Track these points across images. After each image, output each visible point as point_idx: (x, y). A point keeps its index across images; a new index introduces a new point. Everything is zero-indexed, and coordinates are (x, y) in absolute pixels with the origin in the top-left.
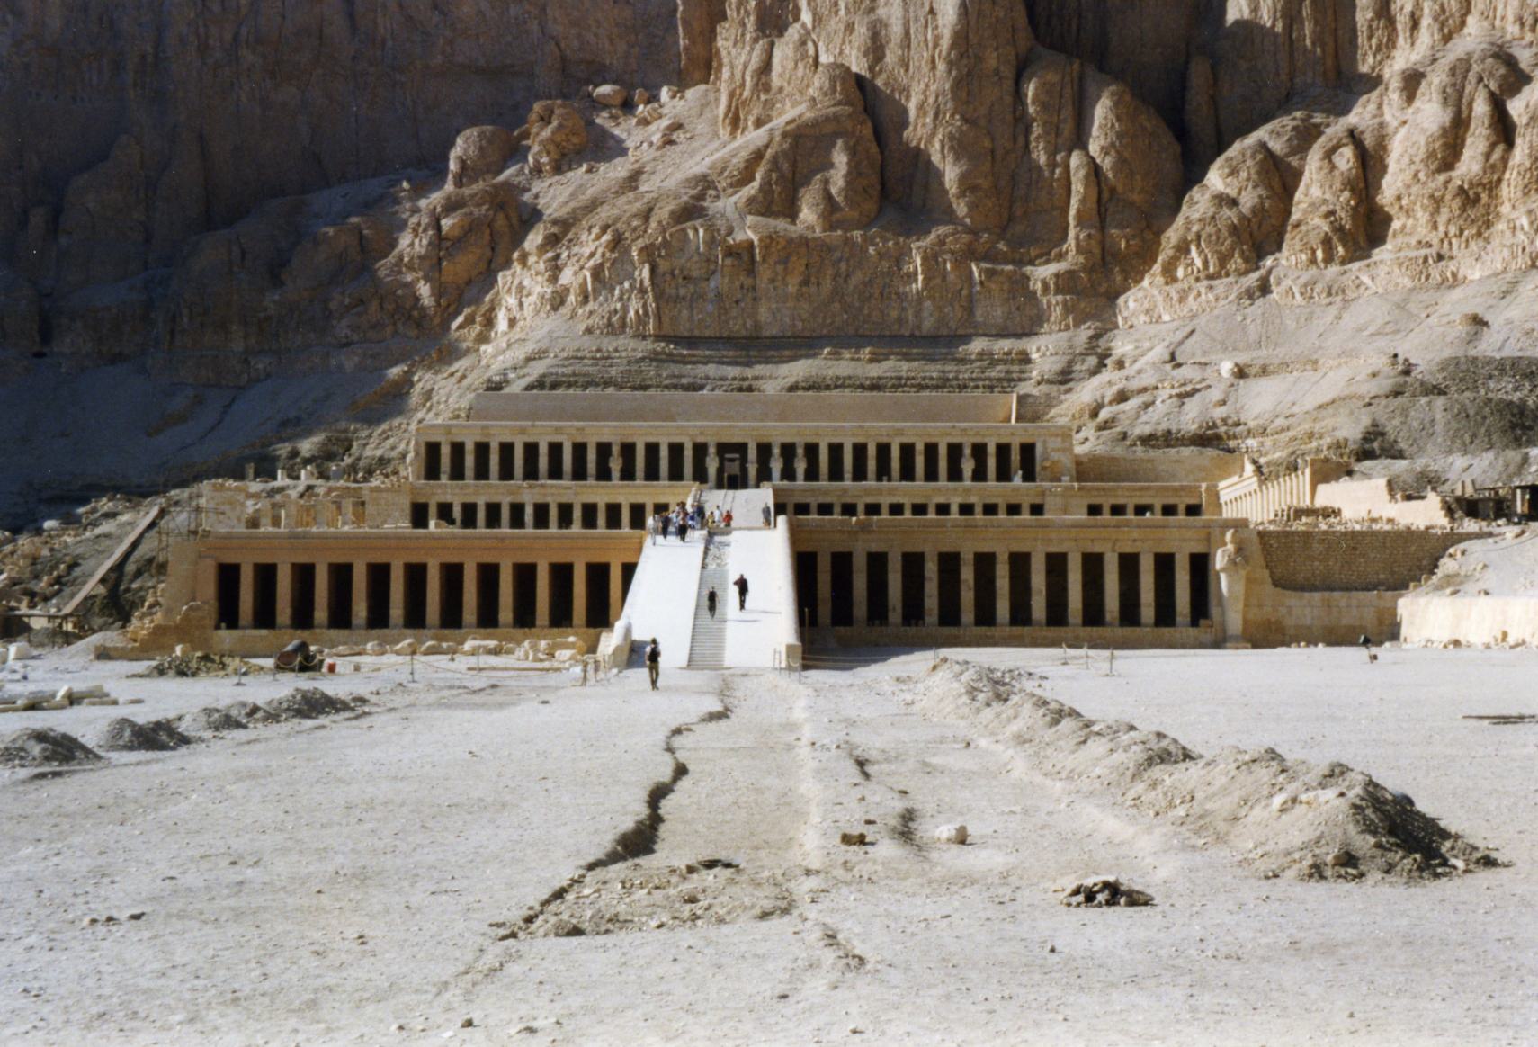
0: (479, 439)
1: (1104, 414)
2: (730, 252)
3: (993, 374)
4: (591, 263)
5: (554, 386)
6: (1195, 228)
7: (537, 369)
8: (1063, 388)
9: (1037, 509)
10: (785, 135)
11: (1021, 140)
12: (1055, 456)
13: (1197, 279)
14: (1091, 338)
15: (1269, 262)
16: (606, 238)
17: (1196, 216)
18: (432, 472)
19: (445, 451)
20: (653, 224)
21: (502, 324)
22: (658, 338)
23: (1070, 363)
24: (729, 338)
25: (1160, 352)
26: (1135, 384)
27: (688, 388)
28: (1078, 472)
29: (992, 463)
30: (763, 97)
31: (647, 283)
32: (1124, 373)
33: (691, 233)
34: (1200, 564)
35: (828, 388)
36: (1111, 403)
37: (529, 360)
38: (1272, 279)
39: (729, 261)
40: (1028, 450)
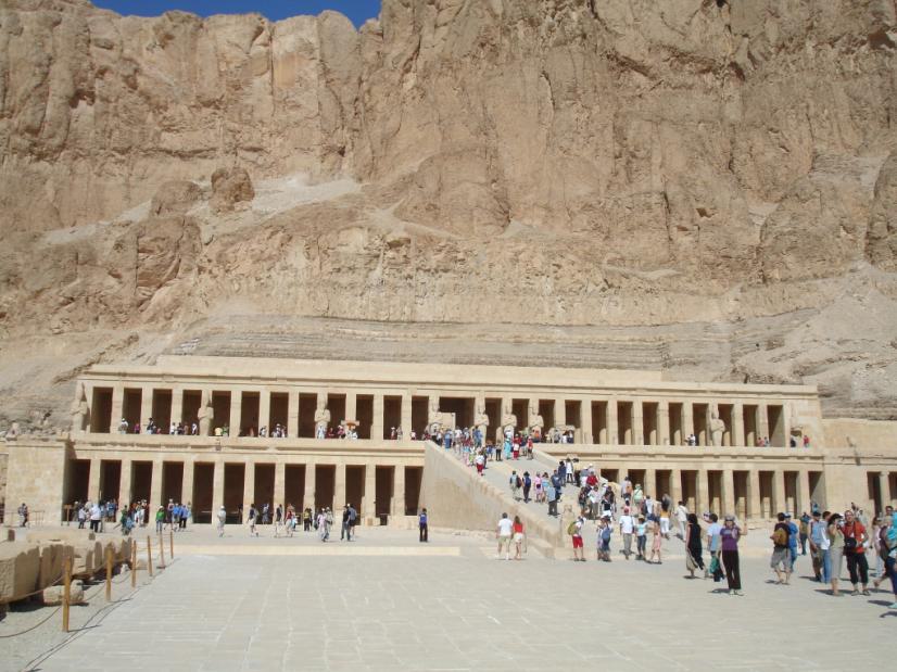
0: (159, 386)
5: (229, 355)
7: (214, 344)
10: (431, 160)
11: (623, 173)
12: (801, 421)
13: (801, 279)
16: (281, 234)
19: (118, 399)
24: (388, 321)
28: (826, 438)
29: (739, 424)
30: (396, 152)
31: (316, 272)
37: (207, 335)
39: (390, 254)
40: (774, 412)
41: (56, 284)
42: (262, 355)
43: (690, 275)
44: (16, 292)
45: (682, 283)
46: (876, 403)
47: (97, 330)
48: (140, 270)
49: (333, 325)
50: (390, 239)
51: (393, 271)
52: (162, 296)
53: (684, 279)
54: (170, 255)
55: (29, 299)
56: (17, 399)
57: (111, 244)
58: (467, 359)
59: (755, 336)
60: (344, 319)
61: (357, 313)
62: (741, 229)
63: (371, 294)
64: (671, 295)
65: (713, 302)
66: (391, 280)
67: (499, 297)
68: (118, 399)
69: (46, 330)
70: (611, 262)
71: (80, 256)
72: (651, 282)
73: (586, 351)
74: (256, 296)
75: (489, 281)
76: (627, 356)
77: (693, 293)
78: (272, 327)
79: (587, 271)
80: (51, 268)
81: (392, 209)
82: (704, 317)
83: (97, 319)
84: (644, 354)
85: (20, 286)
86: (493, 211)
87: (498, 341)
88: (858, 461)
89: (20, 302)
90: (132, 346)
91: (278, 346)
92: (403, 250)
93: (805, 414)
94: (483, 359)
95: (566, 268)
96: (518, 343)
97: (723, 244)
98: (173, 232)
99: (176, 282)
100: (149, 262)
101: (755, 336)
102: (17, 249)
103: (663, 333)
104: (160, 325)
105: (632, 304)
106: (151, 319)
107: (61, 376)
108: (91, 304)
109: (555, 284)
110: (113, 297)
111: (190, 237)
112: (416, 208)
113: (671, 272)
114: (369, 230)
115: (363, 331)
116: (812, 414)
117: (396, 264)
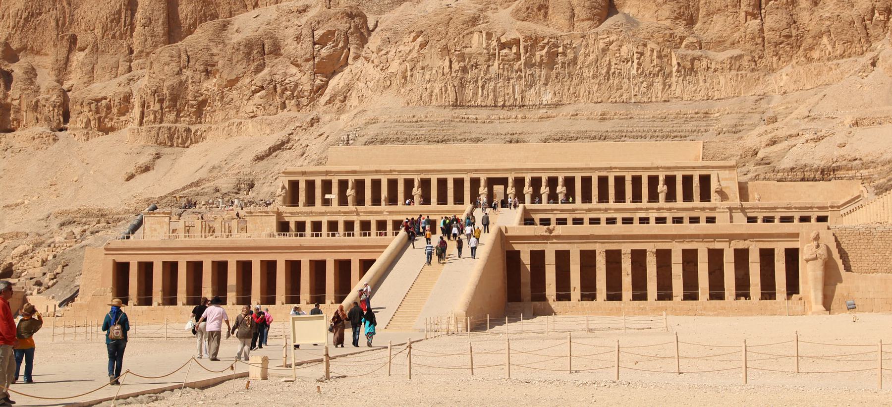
0: (324, 178)
1: (760, 155)
2: (503, 46)
3: (688, 128)
4: (410, 57)
5: (383, 142)
6: (828, 23)
7: (372, 131)
8: (737, 136)
9: (711, 220)
12: (724, 184)
13: (829, 59)
14: (757, 101)
15: (878, 45)
16: (420, 39)
17: (828, 15)
18: (293, 200)
19: (302, 186)
20: (451, 30)
21: (353, 101)
22: (455, 106)
23: (743, 118)
24: (504, 106)
25: (803, 110)
26: (782, 133)
27: (476, 141)
31: (447, 70)
32: (776, 125)
33: (476, 36)
34: (792, 256)
35: (571, 139)
36: (768, 145)
37: (367, 124)
38: (880, 57)
39: (504, 52)
40: (705, 180)
41: (248, 73)
42: (404, 142)
43: (753, 54)
44: (215, 80)
45: (745, 62)
46: (793, 168)
47: (283, 114)
48: (316, 60)
49: (461, 112)
50: (503, 40)
51: (507, 66)
52: (337, 82)
53: (745, 58)
54: (340, 45)
55: (226, 86)
56: (226, 176)
57: (291, 32)
58: (559, 136)
59: (787, 108)
60: (469, 106)
61: (479, 102)
62: (805, 8)
63: (492, 84)
64: (734, 72)
65: (771, 78)
66: (505, 73)
67: (592, 81)
68: (302, 186)
69: (243, 114)
70: (687, 47)
71: (266, 47)
72: (717, 63)
73: (655, 124)
74: (403, 90)
75: (585, 70)
76: (690, 126)
77: (753, 70)
78: (414, 117)
79: (666, 56)
80: (242, 59)
81: (510, 10)
82: (759, 90)
83: (284, 103)
84: (704, 124)
85: (217, 76)
86: (591, 8)
87: (588, 119)
88: (743, 210)
89: (219, 90)
90: (315, 125)
91: (416, 133)
92: (514, 50)
93: (726, 179)
94: (572, 135)
95: (648, 53)
96: (603, 118)
97: (784, 23)
98: (342, 25)
99: (347, 70)
100: (324, 52)
101: (787, 108)
102: (211, 40)
103: (718, 105)
104: (335, 108)
105: (701, 81)
106: (329, 102)
107: (260, 154)
108: (279, 90)
109: (638, 69)
110: (296, 85)
111: (356, 27)
112: (528, 8)
113: (736, 52)
114: (487, 34)
115: (483, 114)
116: (731, 179)
117: (509, 61)
